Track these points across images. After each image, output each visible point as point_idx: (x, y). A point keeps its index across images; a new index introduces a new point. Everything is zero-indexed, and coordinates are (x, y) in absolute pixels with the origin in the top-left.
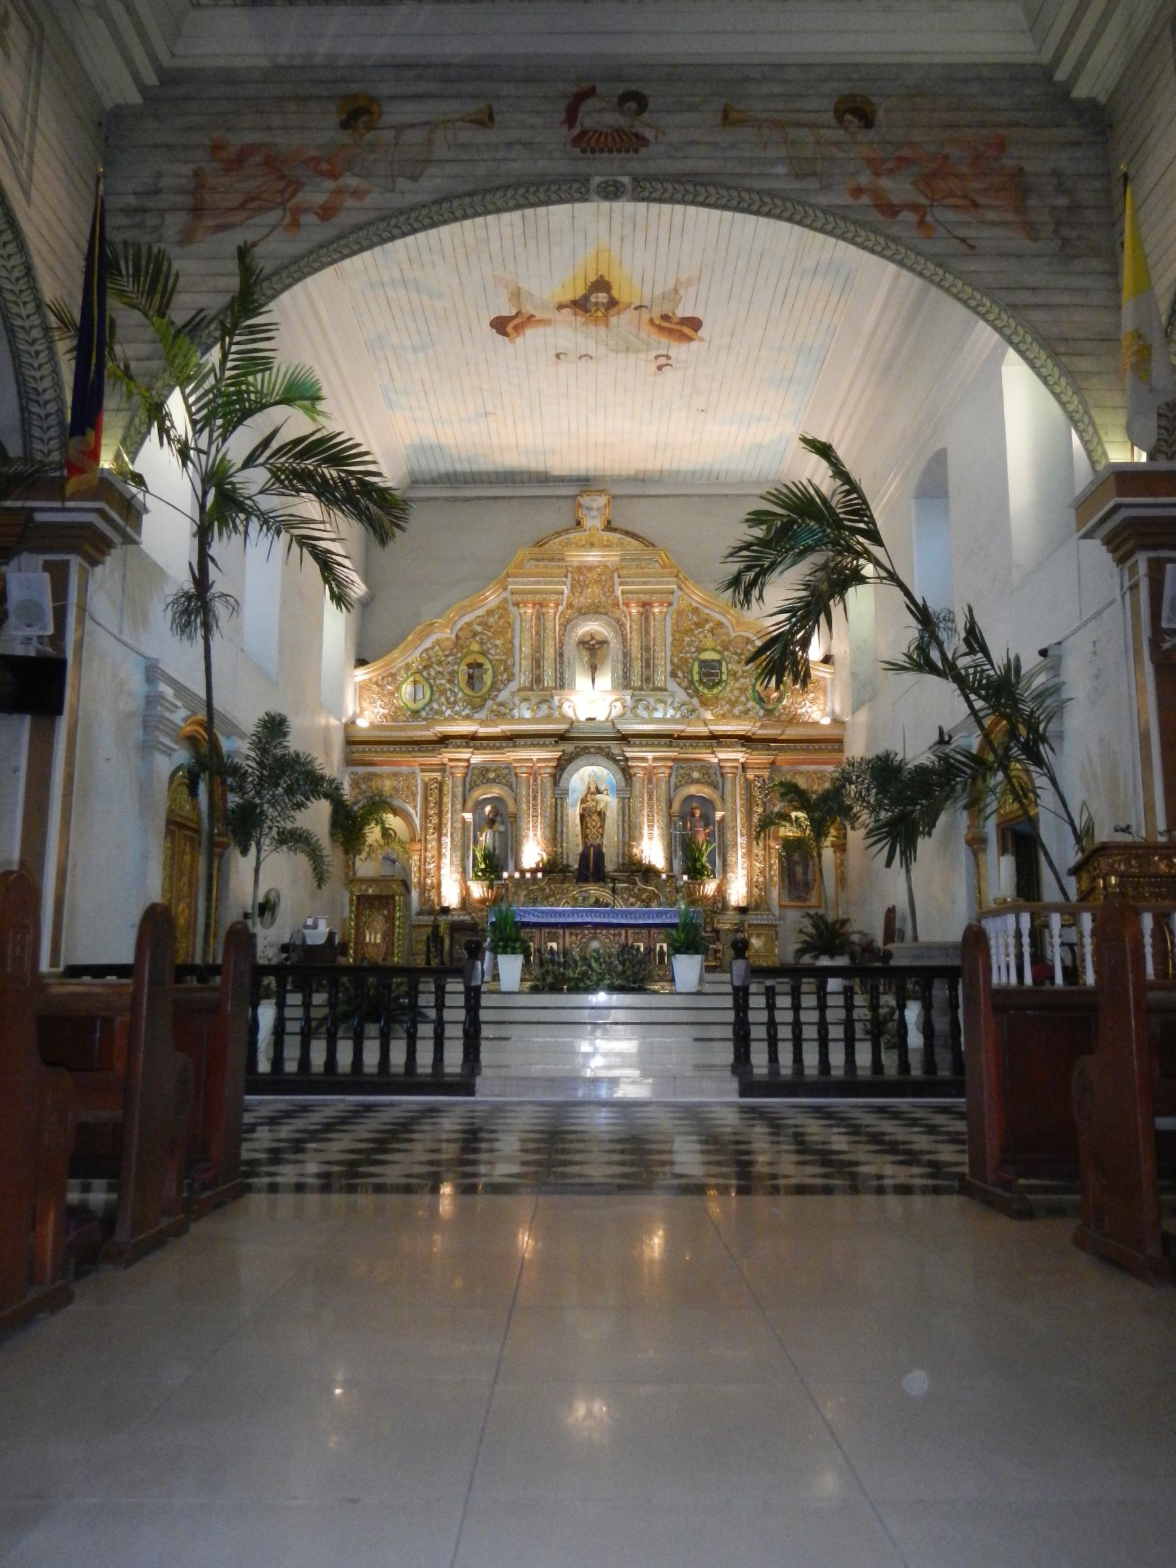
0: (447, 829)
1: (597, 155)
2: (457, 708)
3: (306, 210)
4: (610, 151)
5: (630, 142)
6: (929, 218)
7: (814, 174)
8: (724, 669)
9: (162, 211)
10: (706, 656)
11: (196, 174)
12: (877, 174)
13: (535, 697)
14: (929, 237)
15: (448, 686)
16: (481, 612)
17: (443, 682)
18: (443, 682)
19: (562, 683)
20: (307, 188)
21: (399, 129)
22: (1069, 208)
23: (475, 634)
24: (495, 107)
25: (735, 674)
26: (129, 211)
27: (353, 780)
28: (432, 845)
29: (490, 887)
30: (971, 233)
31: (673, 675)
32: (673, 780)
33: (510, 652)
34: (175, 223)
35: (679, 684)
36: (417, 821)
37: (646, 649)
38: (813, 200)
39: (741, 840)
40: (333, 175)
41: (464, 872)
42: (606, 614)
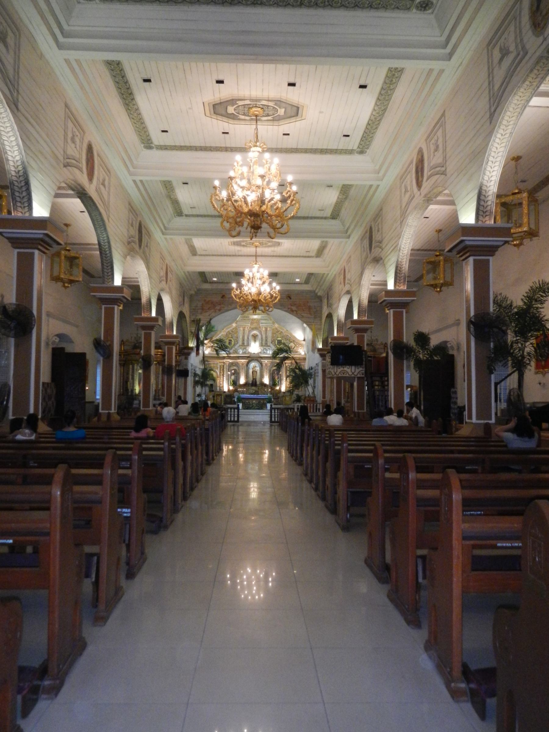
0: (225, 375)
12: (291, 306)
13: (243, 347)
16: (231, 328)
19: (248, 345)
23: (230, 333)
26: (194, 309)
28: (222, 378)
29: (234, 387)
30: (303, 314)
31: (272, 343)
33: (237, 337)
34: (200, 311)
36: (218, 373)
37: (266, 337)
39: (284, 378)
41: (228, 384)
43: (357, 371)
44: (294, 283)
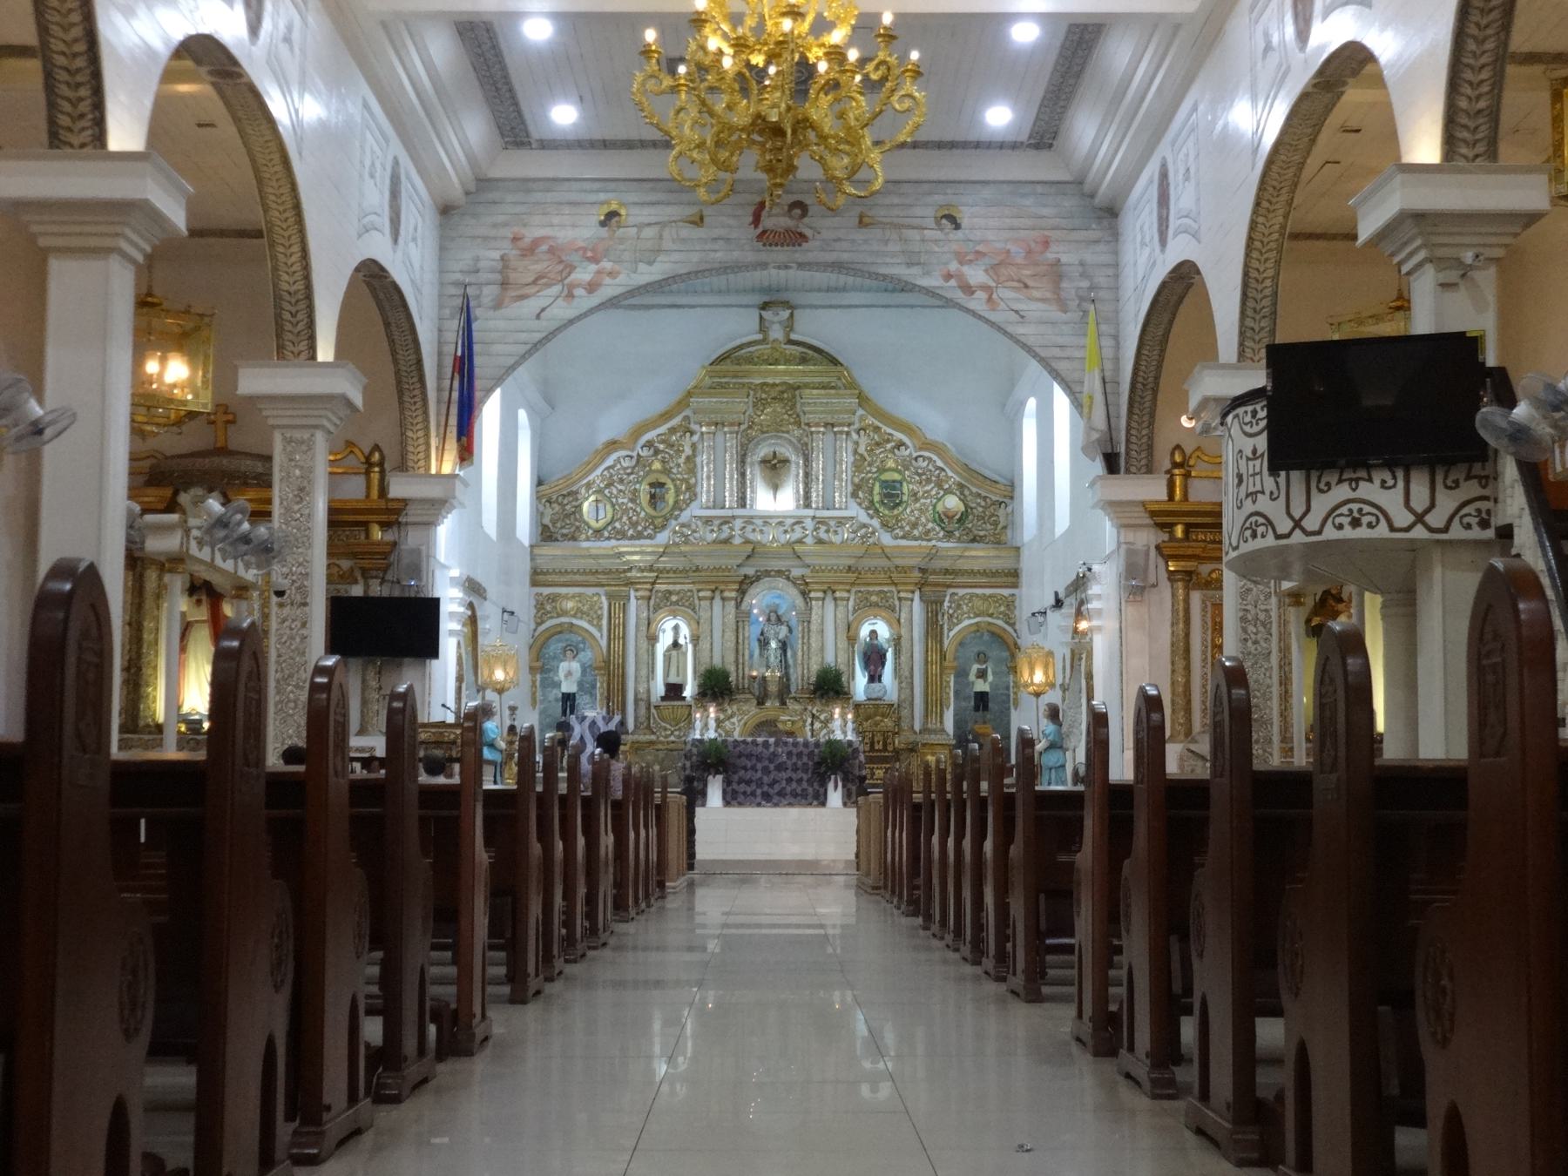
1: (774, 248)
2: (640, 528)
3: (579, 285)
4: (782, 245)
5: (797, 238)
6: (995, 296)
7: (918, 264)
8: (905, 490)
9: (480, 285)
10: (884, 477)
11: (502, 258)
12: (961, 263)
14: (994, 310)
15: (630, 505)
17: (625, 501)
18: (625, 501)
20: (578, 270)
21: (640, 227)
22: (1091, 288)
24: (705, 213)
25: (915, 494)
27: (537, 601)
31: (854, 495)
32: (851, 603)
34: (490, 292)
35: (860, 504)
38: (918, 283)
40: (595, 260)
42: (788, 432)
43: (1447, 503)
44: (978, 145)
